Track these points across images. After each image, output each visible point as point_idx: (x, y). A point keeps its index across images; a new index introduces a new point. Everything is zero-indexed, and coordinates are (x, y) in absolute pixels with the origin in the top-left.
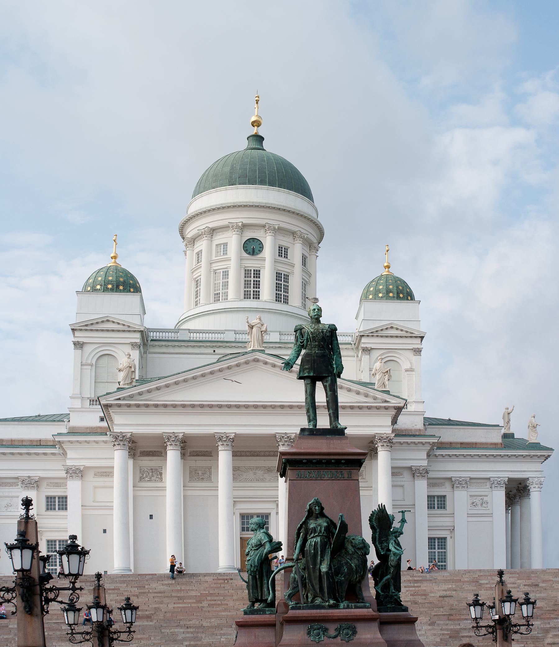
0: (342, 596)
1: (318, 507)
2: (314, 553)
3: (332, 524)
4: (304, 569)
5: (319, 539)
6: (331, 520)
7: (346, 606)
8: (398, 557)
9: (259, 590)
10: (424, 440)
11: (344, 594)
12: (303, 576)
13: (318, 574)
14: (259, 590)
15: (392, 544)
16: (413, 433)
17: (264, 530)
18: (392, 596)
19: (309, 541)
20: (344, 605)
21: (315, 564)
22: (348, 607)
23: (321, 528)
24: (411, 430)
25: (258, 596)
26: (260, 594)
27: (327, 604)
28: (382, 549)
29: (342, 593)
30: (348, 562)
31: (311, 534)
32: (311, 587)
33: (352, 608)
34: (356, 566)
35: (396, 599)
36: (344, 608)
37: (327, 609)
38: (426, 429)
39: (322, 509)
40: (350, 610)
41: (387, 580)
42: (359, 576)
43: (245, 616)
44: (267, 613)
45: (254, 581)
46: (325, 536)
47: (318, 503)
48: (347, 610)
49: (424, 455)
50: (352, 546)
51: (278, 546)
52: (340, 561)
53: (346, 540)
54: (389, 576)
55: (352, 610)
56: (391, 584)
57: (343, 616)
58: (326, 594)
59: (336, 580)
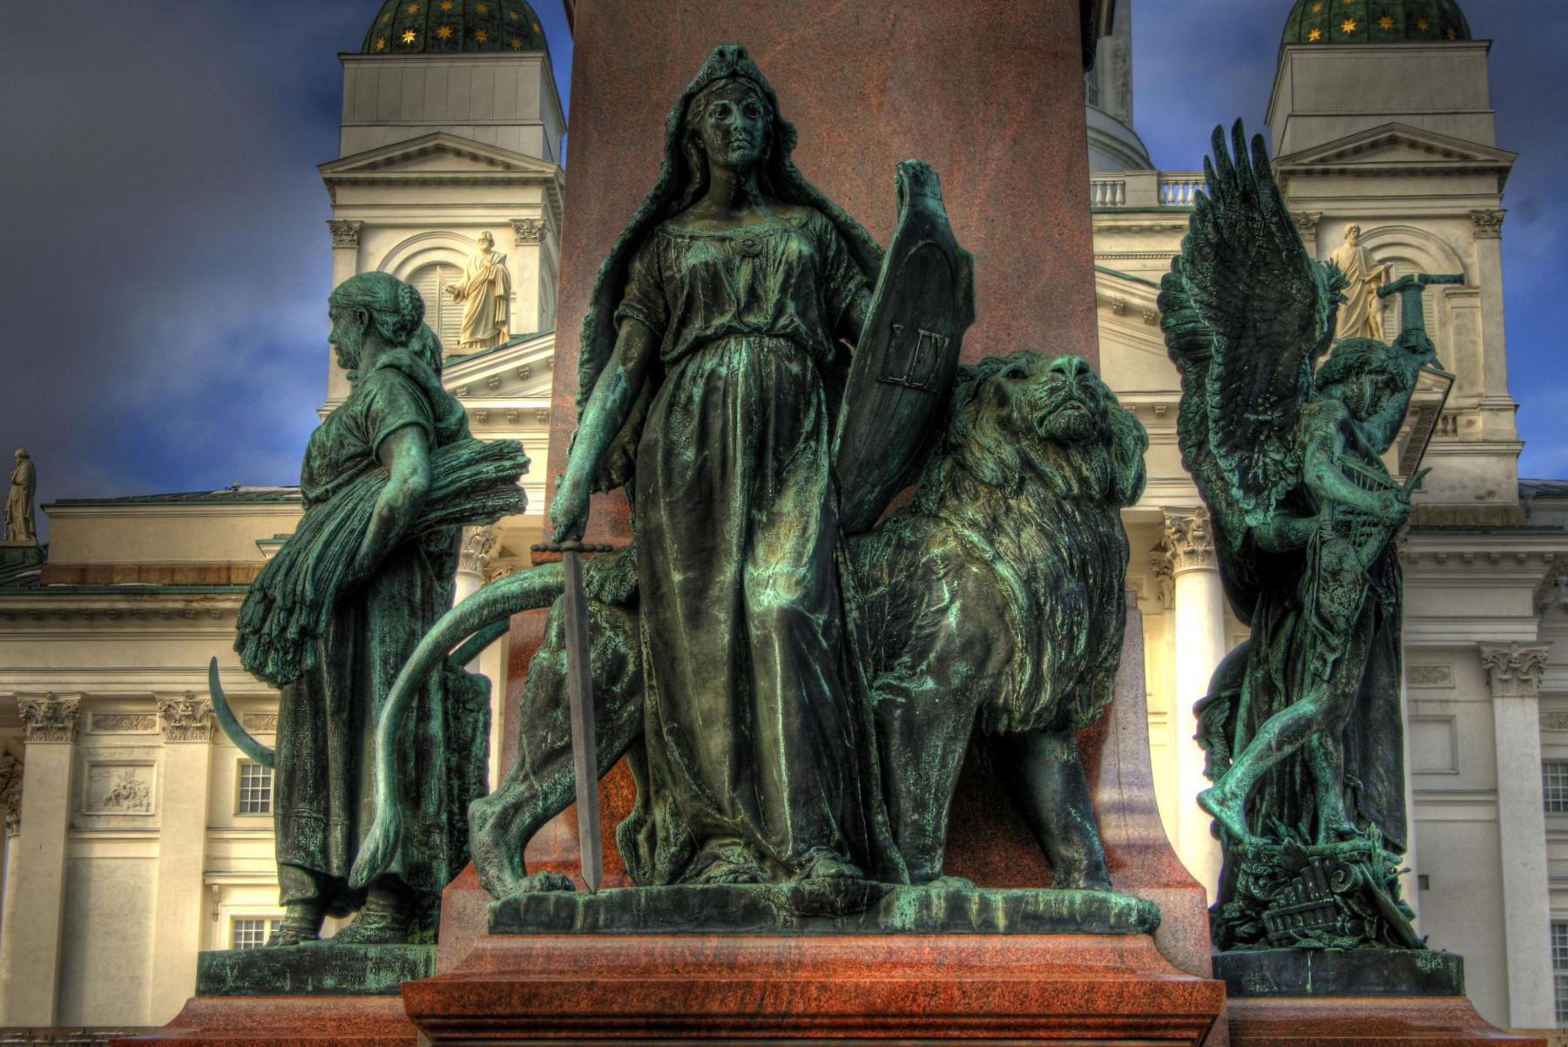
0: (920, 830)
1: (749, 112)
2: (702, 469)
3: (843, 246)
4: (630, 604)
5: (738, 359)
6: (844, 230)
7: (939, 908)
8: (1370, 549)
9: (336, 805)
10: (1523, 547)
11: (936, 819)
12: (620, 661)
13: (723, 634)
14: (336, 805)
15: (1325, 444)
16: (1482, 521)
17: (402, 355)
18: (1334, 867)
19: (673, 374)
20: (925, 904)
21: (703, 556)
22: (956, 918)
23: (757, 276)
24: (1473, 511)
25: (325, 849)
26: (337, 834)
27: (785, 886)
28: (1253, 488)
29: (921, 806)
30: (970, 554)
31: (684, 322)
32: (675, 754)
33: (988, 928)
34: (1029, 581)
35: (1366, 894)
36: (923, 928)
37: (786, 931)
38: (1528, 511)
39: (779, 137)
40: (970, 942)
41: (1298, 730)
42: (1061, 672)
43: (207, 1002)
44: (372, 982)
45: (306, 735)
46: (792, 337)
47: (739, 75)
48: (949, 942)
49: (1522, 602)
50: (1005, 424)
51: (488, 469)
52: (914, 547)
53: (961, 391)
54: (1306, 706)
55: (993, 943)
56: (1326, 775)
57: (912, 991)
58: (784, 812)
59: (876, 697)
